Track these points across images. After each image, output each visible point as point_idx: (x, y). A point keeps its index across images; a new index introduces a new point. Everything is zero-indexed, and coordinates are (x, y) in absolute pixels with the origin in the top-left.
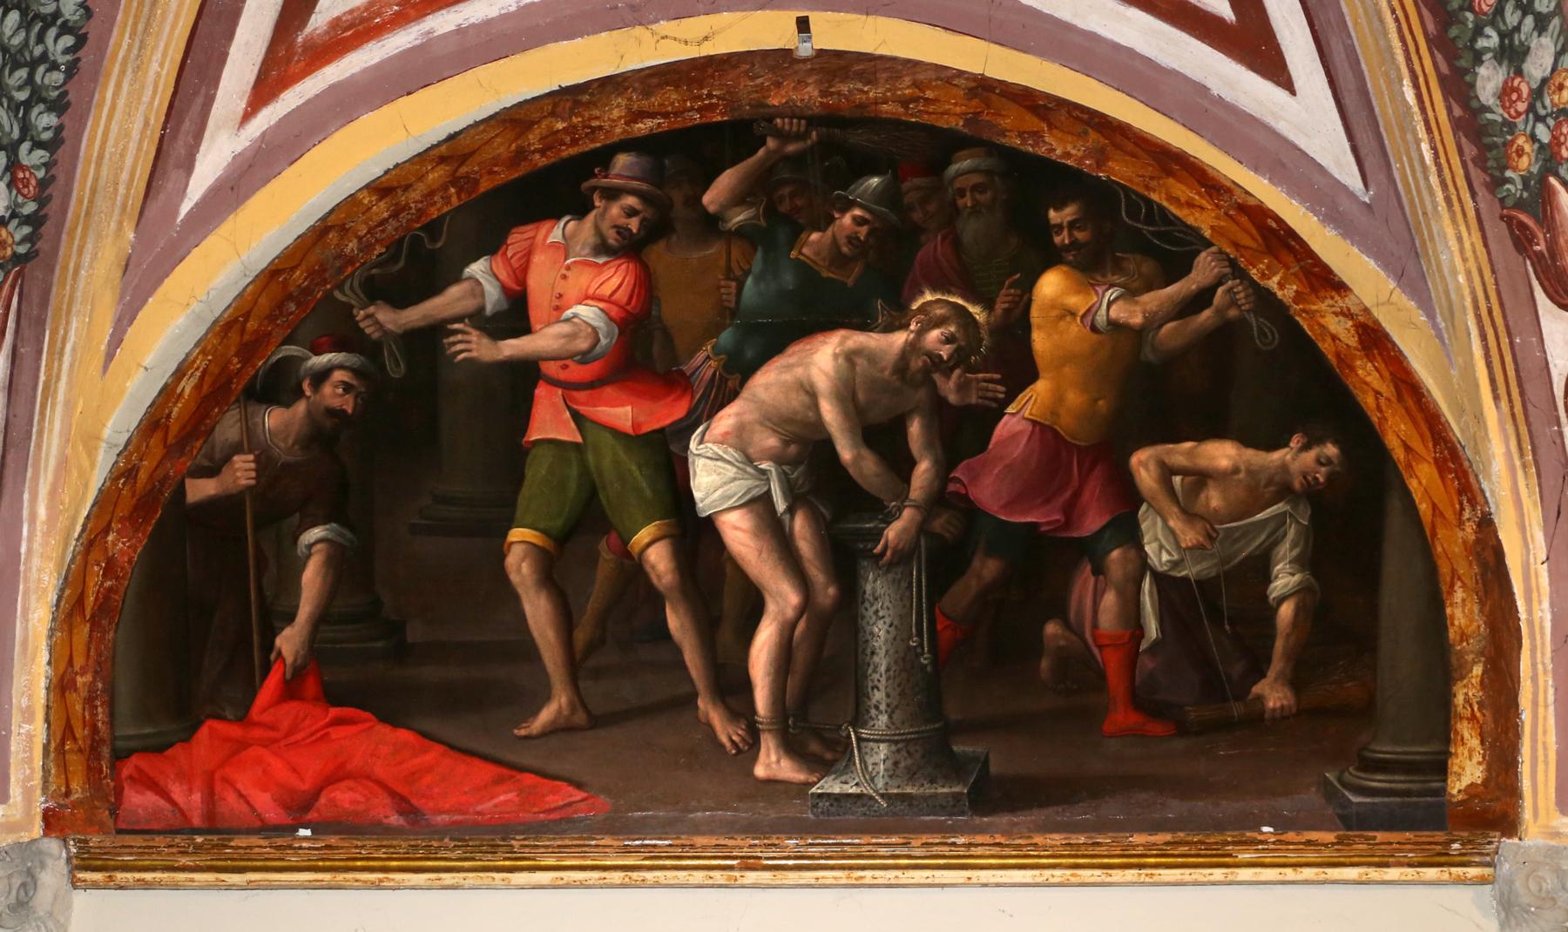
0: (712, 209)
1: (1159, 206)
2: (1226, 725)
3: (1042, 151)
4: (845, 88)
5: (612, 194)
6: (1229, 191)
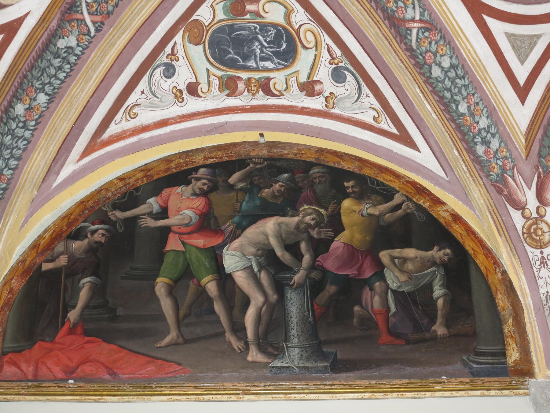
0: (231, 183)
1: (381, 182)
2: (425, 340)
3: (341, 167)
4: (275, 151)
5: (198, 179)
6: (403, 177)
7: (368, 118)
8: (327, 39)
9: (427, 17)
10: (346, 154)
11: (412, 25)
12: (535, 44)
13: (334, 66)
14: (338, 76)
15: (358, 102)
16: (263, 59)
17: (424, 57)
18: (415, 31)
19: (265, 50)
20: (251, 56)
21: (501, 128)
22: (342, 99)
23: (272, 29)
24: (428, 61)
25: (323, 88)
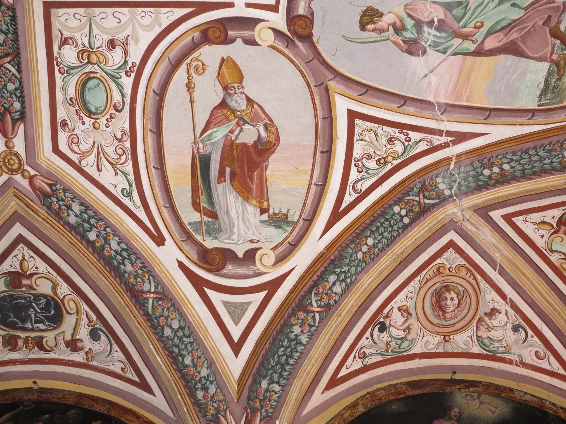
1: (123, 421)
3: (94, 409)
4: (44, 396)
6: (142, 418)
7: (117, 369)
8: (85, 307)
9: (160, 290)
10: (100, 398)
11: (148, 295)
12: (246, 309)
13: (91, 328)
14: (94, 335)
15: (110, 356)
16: (37, 322)
17: (158, 321)
18: (151, 301)
19: (38, 315)
20: (27, 320)
21: (218, 377)
22: (98, 353)
23: (43, 298)
24: (161, 324)
25: (83, 345)
